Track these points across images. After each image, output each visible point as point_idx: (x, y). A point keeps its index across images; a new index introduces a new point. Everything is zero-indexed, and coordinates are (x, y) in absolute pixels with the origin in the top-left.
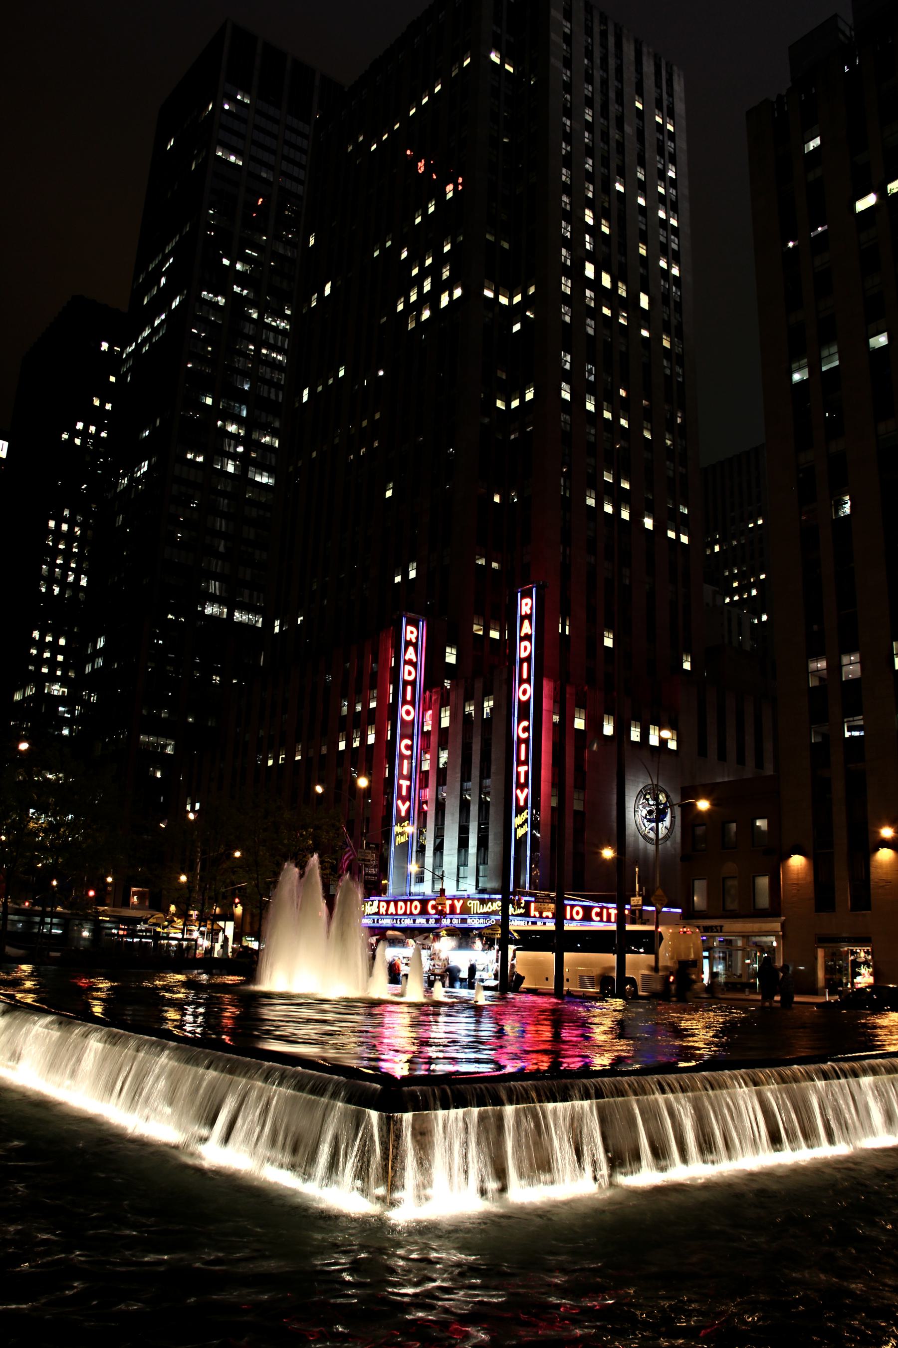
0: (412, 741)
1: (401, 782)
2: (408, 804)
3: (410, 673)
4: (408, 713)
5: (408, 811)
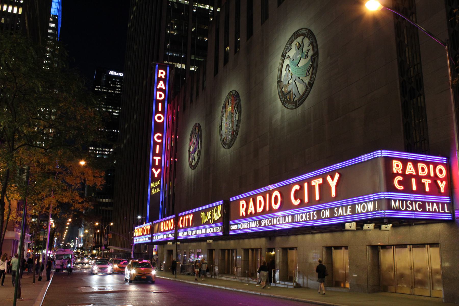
0: (162, 134)
1: (155, 158)
2: (159, 170)
3: (160, 96)
4: (159, 118)
5: (159, 174)
